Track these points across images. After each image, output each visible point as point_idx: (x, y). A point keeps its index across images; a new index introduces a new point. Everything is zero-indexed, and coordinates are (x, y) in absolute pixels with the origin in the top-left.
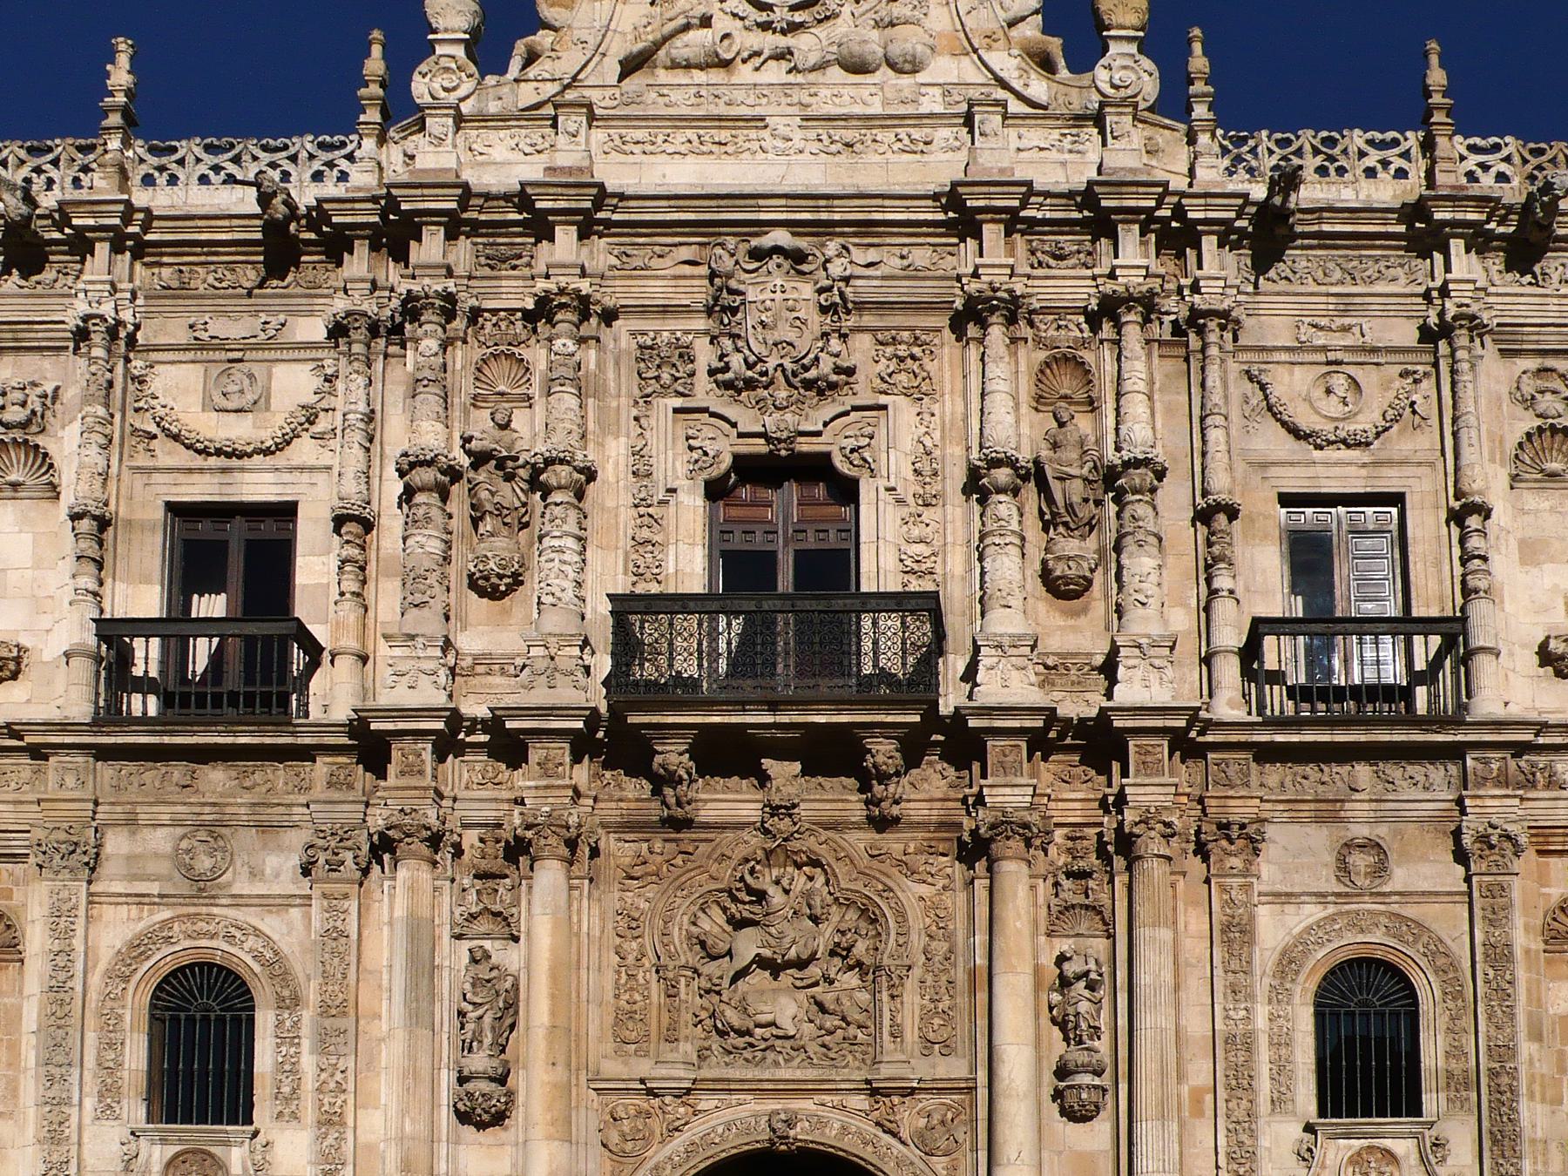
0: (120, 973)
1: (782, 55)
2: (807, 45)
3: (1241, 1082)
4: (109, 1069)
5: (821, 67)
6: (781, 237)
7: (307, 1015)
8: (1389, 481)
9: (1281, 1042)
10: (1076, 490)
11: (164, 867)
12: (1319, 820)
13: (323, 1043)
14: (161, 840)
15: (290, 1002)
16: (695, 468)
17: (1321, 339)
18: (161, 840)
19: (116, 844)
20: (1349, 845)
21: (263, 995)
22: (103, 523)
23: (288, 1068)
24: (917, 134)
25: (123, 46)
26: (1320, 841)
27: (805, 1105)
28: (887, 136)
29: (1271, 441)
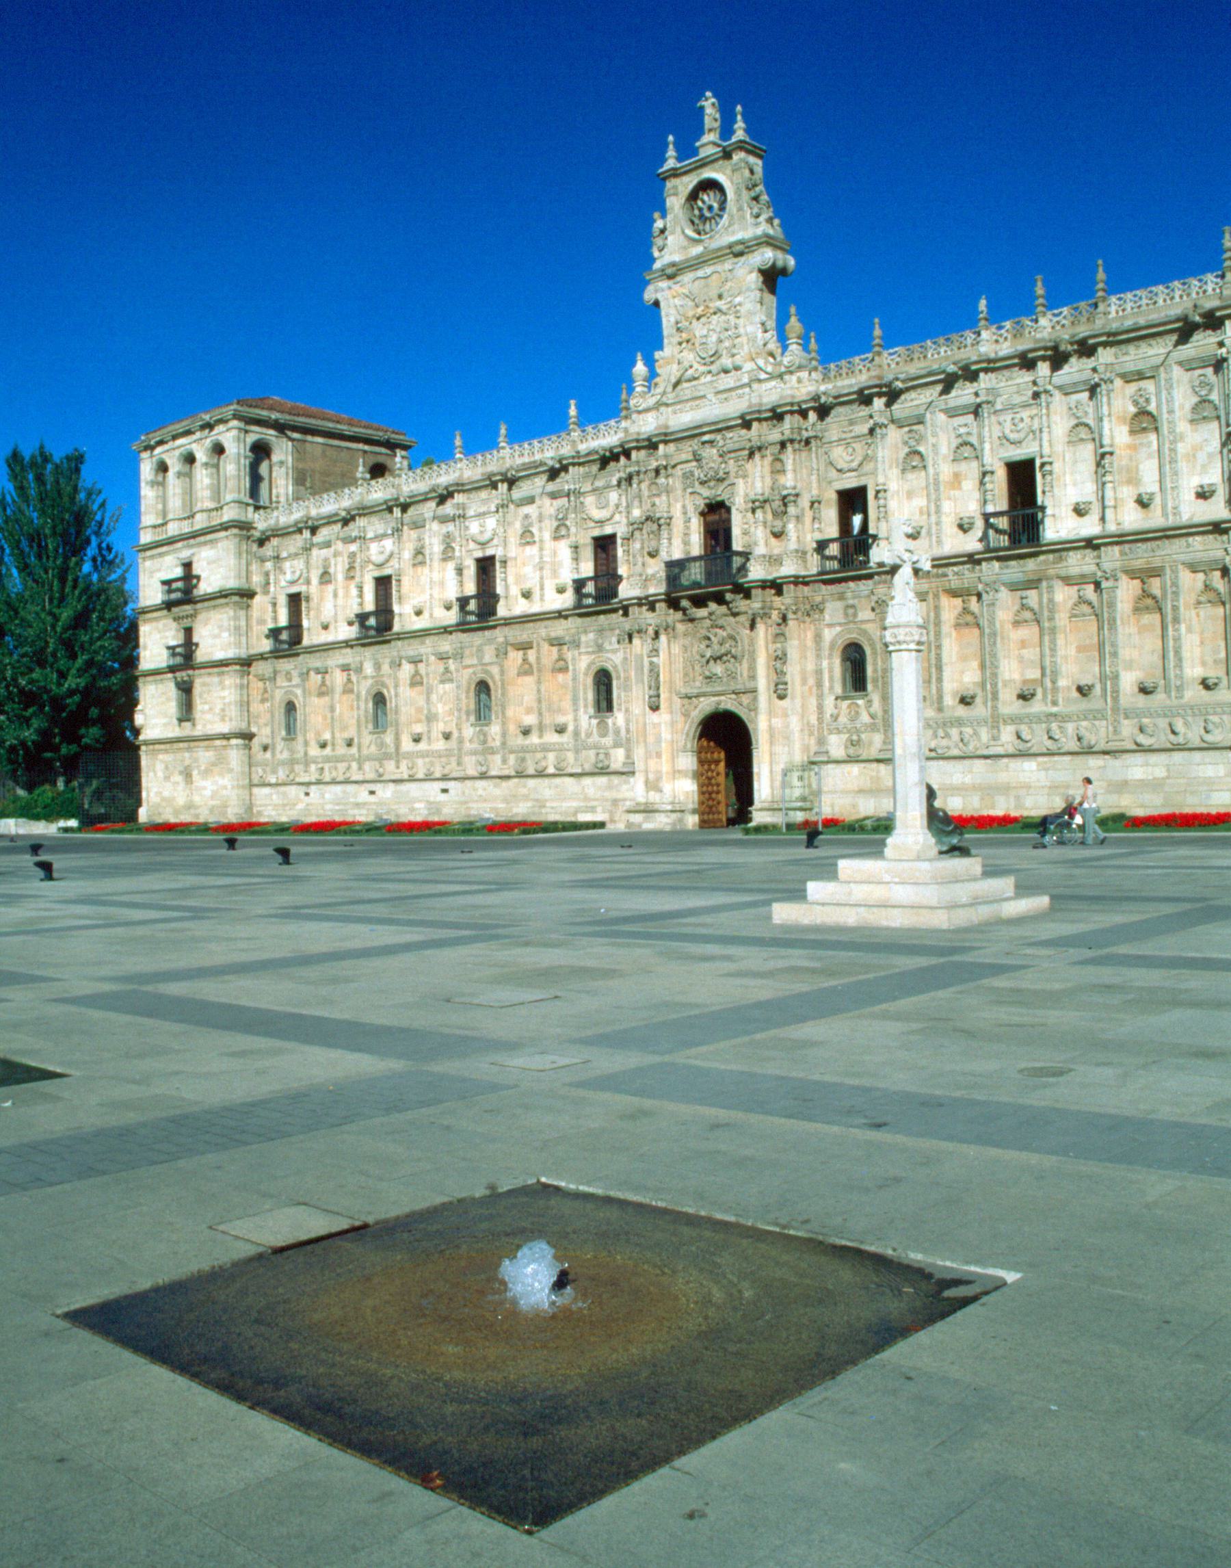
0: (586, 674)
1: (710, 372)
2: (714, 368)
3: (819, 684)
4: (586, 699)
5: (718, 374)
6: (706, 438)
9: (831, 671)
16: (696, 509)
17: (844, 436)
18: (591, 636)
19: (583, 638)
20: (848, 607)
21: (614, 675)
22: (576, 547)
24: (740, 391)
25: (572, 402)
26: (839, 605)
27: (723, 698)
28: (733, 393)
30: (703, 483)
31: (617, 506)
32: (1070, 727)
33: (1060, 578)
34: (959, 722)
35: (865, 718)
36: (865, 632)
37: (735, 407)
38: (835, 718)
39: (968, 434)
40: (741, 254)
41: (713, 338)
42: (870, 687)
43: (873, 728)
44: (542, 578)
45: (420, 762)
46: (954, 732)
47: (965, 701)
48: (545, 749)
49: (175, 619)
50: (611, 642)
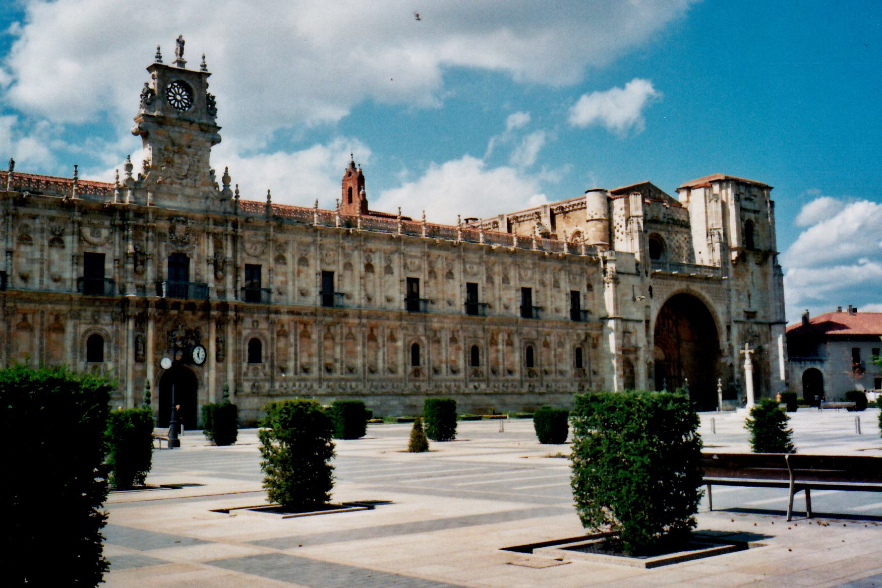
0: (83, 336)
2: (184, 182)
3: (240, 357)
6: (182, 218)
8: (260, 263)
10: (221, 264)
11: (90, 318)
13: (116, 348)
19: (83, 314)
21: (105, 339)
23: (109, 352)
29: (245, 255)
32: (348, 384)
34: (304, 380)
35: (261, 374)
36: (261, 335)
38: (246, 374)
41: (186, 167)
42: (263, 360)
43: (266, 380)
44: (42, 270)
46: (303, 384)
47: (306, 370)
50: (107, 319)
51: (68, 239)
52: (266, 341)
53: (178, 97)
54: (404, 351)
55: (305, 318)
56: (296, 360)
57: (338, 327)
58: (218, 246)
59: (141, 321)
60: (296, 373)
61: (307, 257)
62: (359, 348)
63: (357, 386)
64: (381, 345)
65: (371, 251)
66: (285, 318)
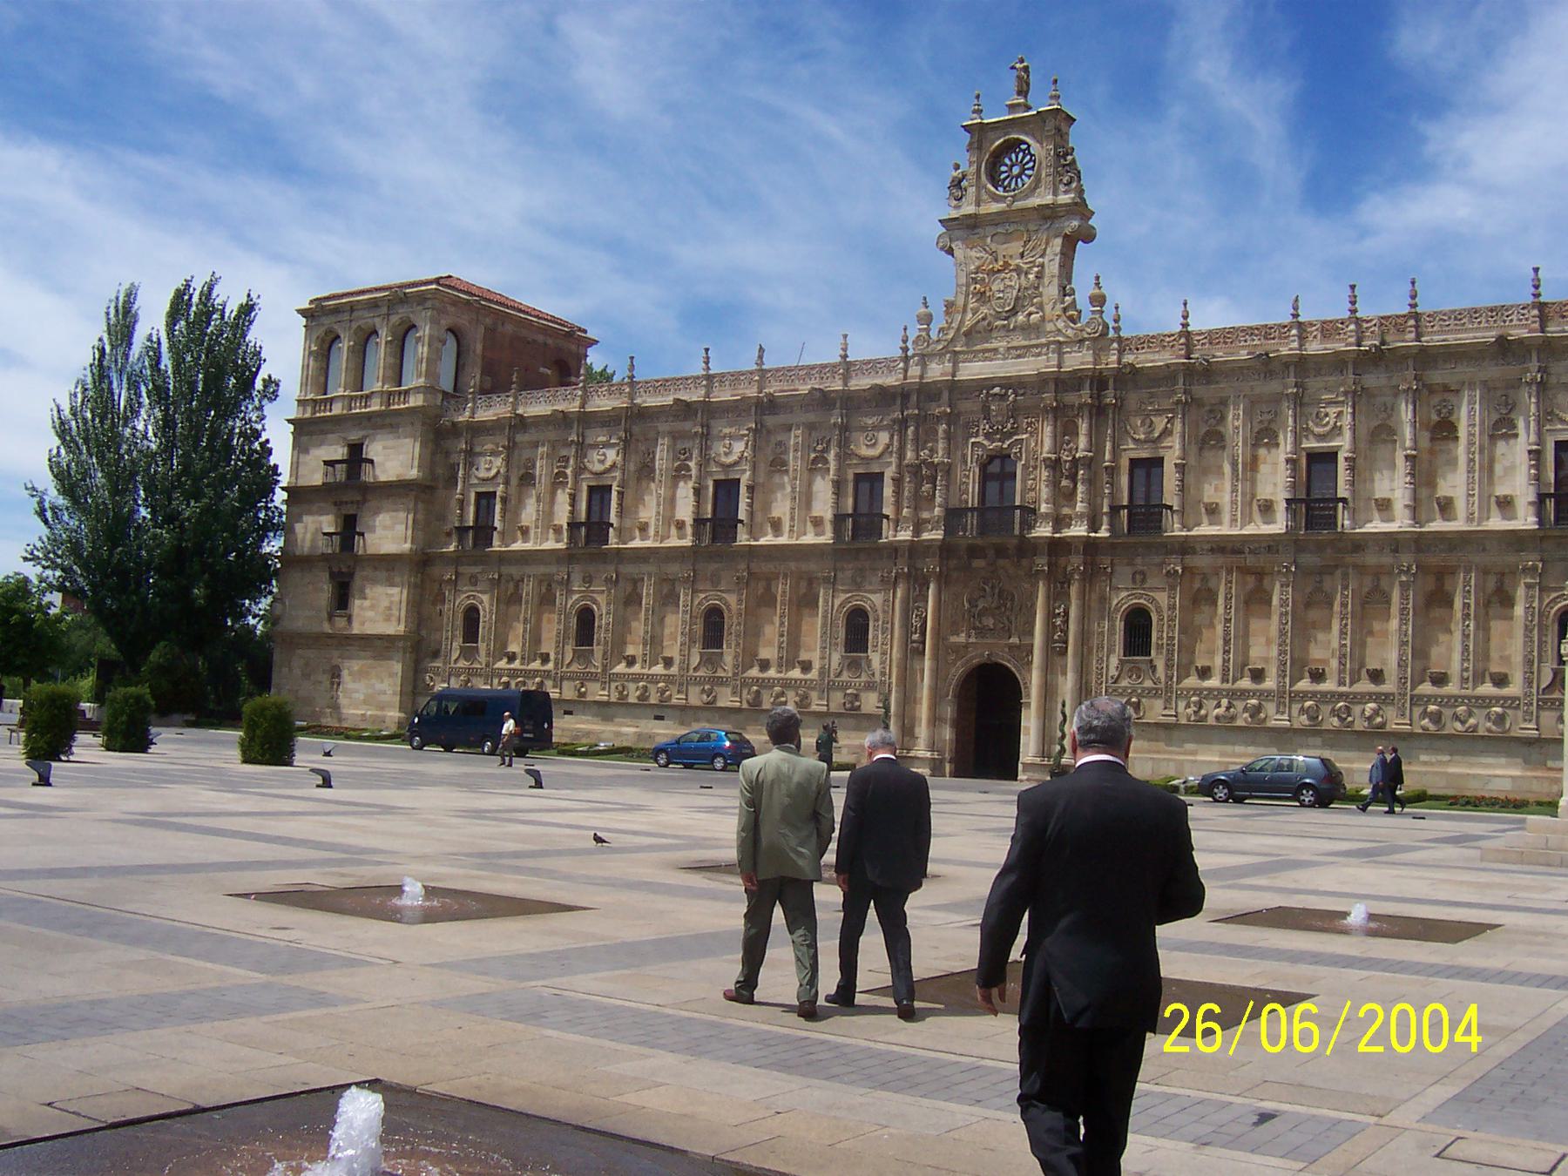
6: (997, 390)
7: (880, 623)
12: (1128, 564)
14: (849, 573)
15: (877, 620)
19: (840, 575)
26: (1128, 570)
30: (987, 436)
31: (888, 446)
32: (1357, 709)
33: (1355, 566)
37: (1028, 367)
39: (1270, 421)
40: (1046, 218)
42: (1153, 652)
45: (632, 686)
46: (1239, 705)
48: (787, 684)
49: (335, 504)
51: (831, 456)
52: (1159, 610)
53: (1016, 170)
54: (1528, 630)
55: (1250, 560)
56: (1226, 652)
57: (1338, 573)
58: (1066, 431)
59: (918, 582)
60: (1225, 680)
61: (1273, 426)
62: (1394, 624)
63: (1376, 713)
64: (1459, 615)
65: (1446, 389)
66: (1202, 561)
